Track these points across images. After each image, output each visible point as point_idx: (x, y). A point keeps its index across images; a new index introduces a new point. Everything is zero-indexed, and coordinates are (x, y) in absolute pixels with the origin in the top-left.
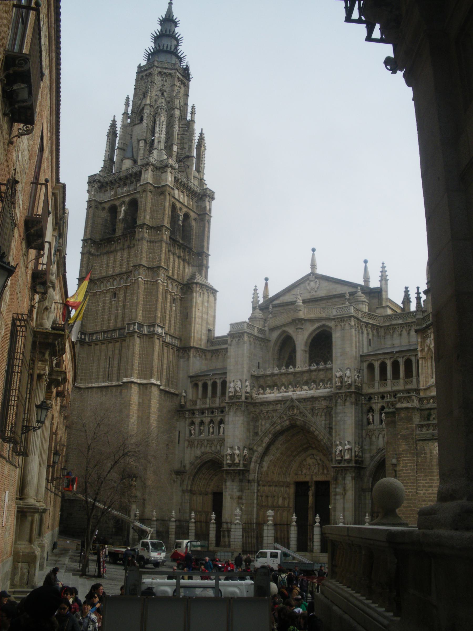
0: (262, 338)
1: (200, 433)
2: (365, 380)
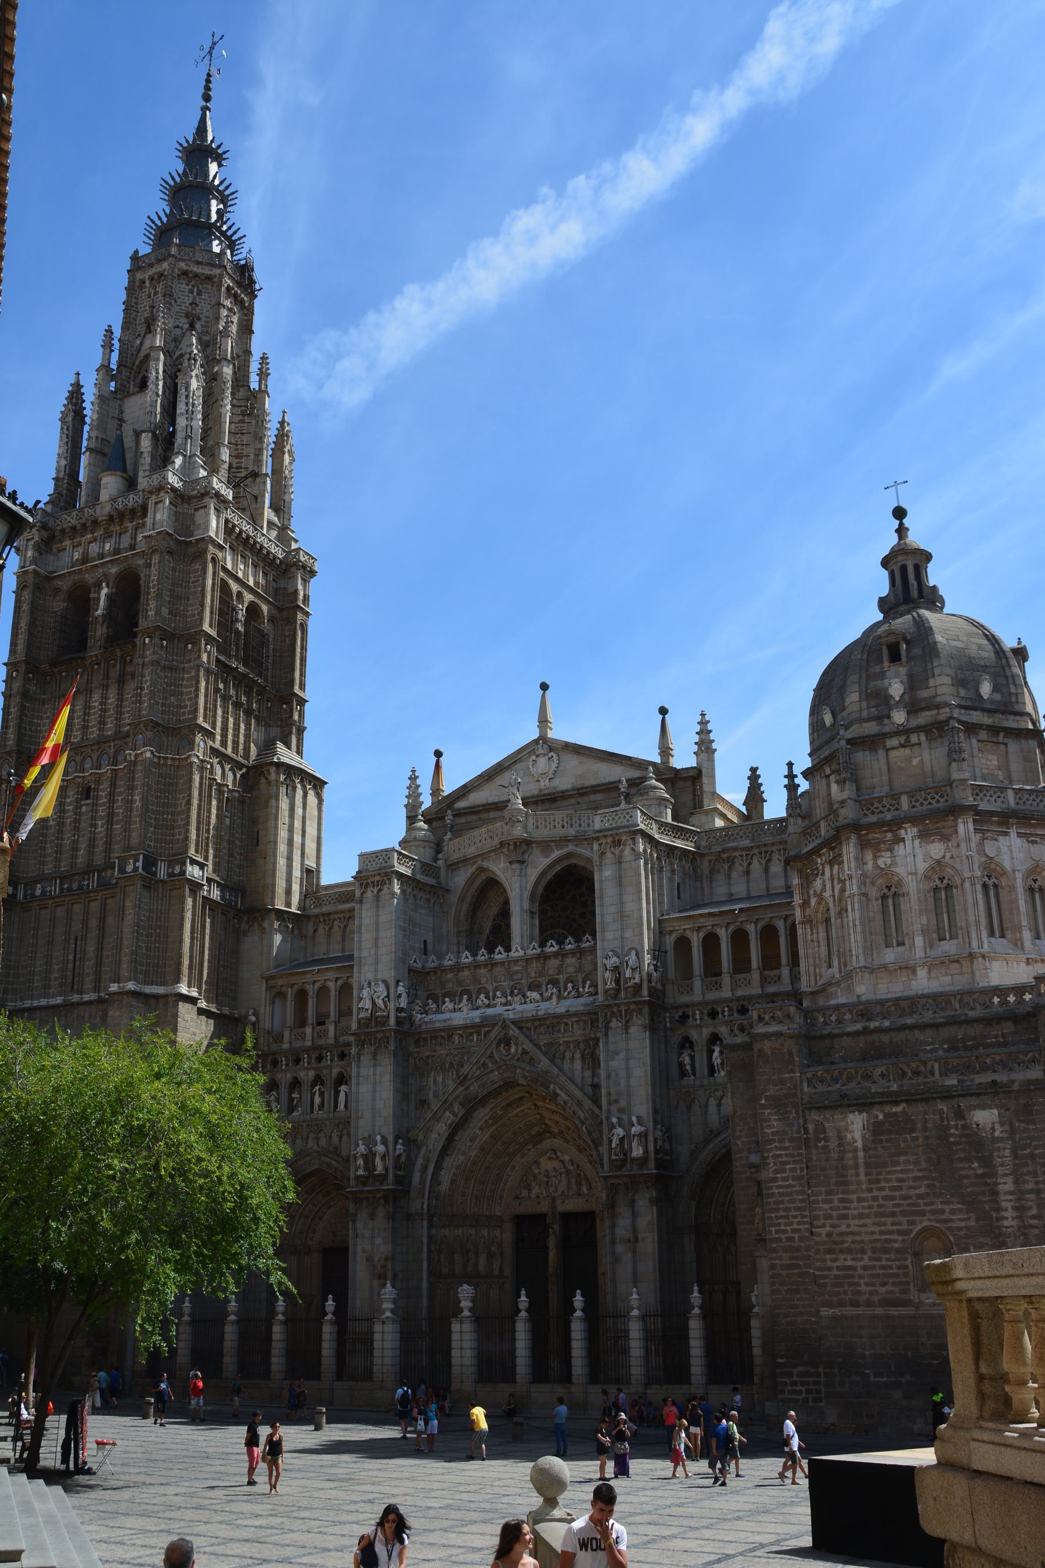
0: (432, 886)
2: (671, 975)
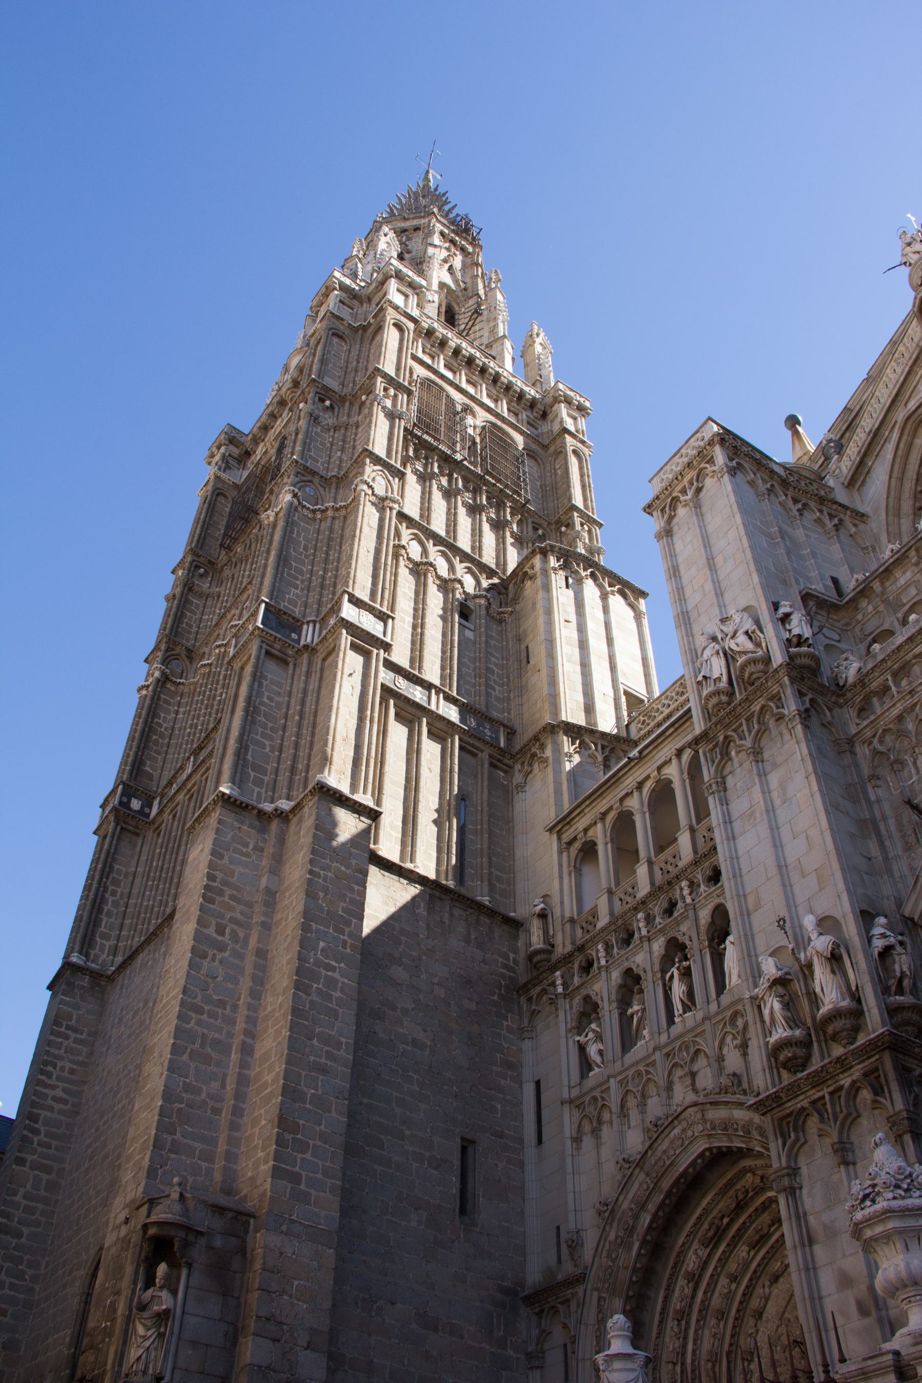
1: (628, 1039)
